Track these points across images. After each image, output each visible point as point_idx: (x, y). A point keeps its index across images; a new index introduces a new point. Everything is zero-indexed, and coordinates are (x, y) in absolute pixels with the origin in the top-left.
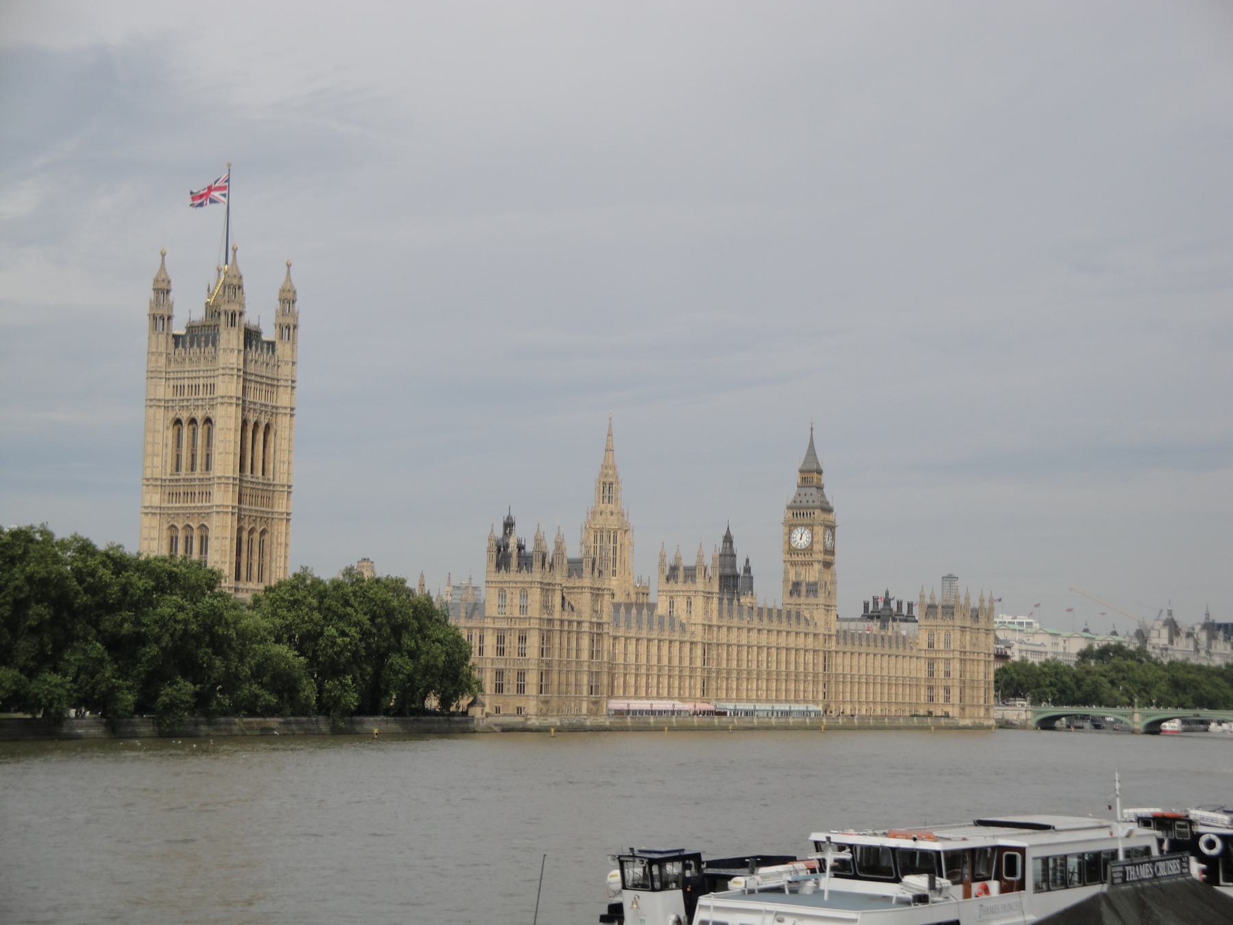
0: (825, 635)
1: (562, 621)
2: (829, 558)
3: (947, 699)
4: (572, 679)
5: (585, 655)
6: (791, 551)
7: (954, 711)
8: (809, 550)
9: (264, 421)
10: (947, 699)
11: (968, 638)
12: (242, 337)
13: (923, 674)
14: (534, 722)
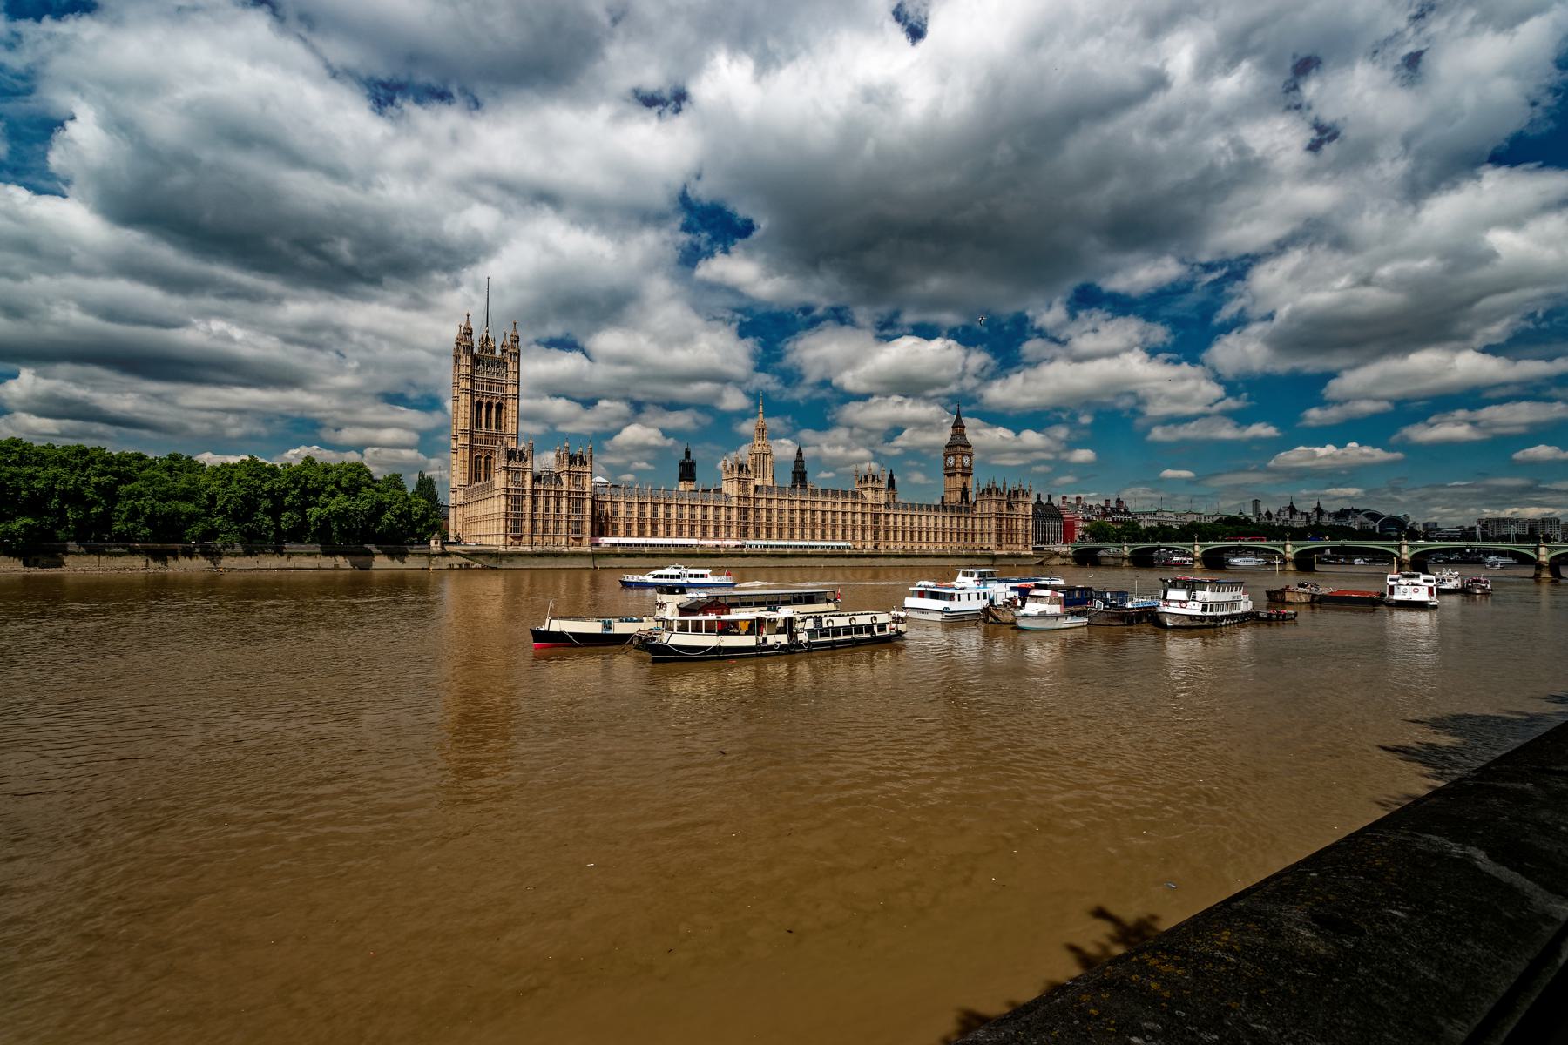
0: (872, 505)
1: (534, 491)
2: (966, 471)
3: (989, 540)
4: (551, 524)
5: (564, 511)
6: (947, 468)
7: (992, 547)
8: (954, 468)
9: (495, 402)
10: (989, 540)
11: (1005, 505)
12: (469, 358)
13: (978, 527)
14: (502, 549)
